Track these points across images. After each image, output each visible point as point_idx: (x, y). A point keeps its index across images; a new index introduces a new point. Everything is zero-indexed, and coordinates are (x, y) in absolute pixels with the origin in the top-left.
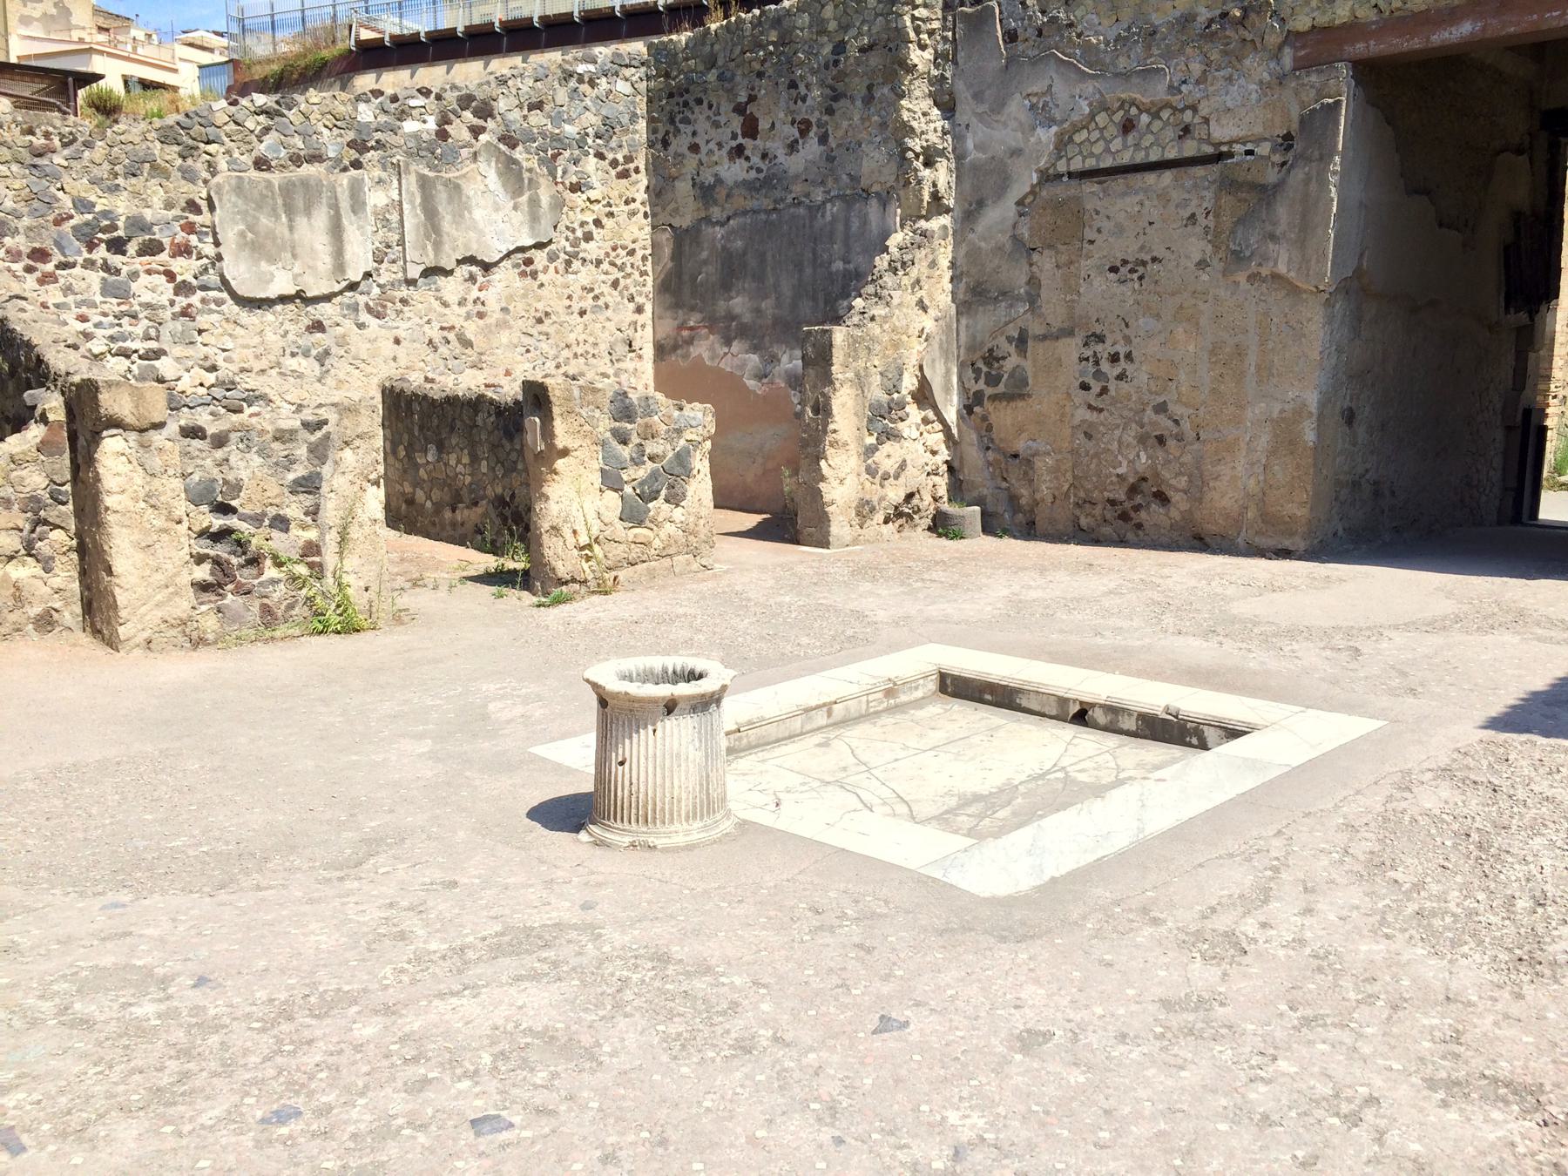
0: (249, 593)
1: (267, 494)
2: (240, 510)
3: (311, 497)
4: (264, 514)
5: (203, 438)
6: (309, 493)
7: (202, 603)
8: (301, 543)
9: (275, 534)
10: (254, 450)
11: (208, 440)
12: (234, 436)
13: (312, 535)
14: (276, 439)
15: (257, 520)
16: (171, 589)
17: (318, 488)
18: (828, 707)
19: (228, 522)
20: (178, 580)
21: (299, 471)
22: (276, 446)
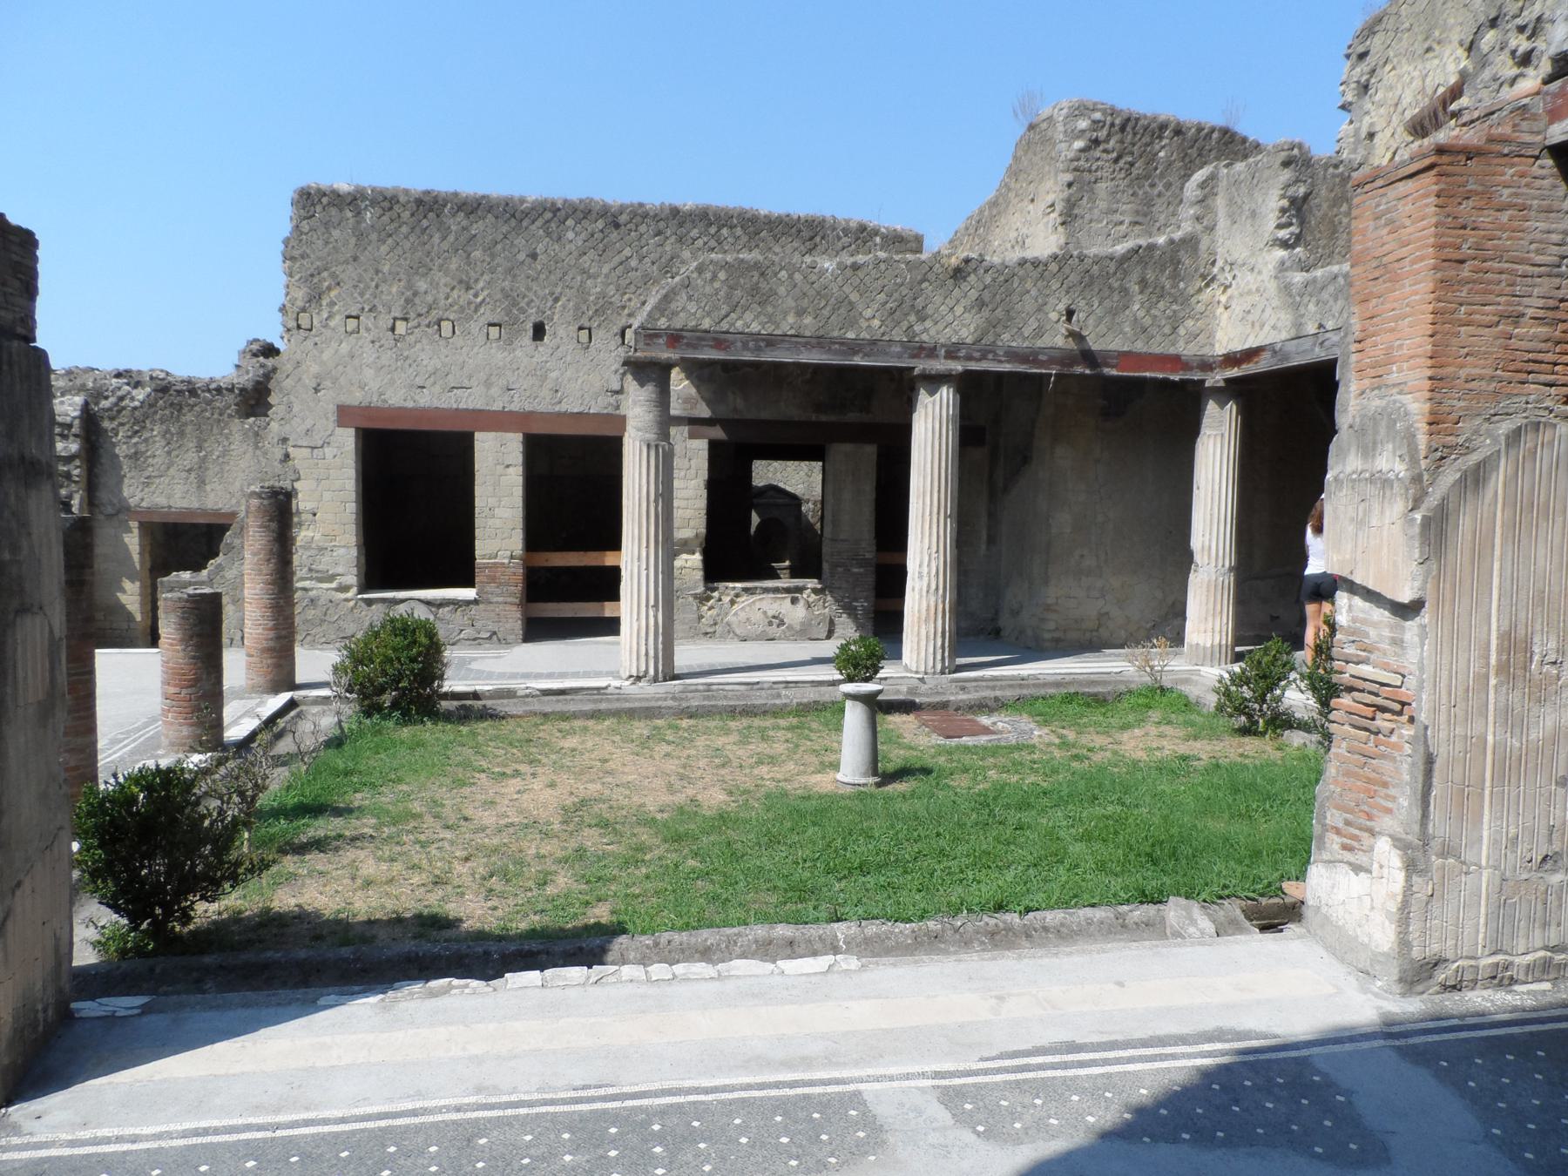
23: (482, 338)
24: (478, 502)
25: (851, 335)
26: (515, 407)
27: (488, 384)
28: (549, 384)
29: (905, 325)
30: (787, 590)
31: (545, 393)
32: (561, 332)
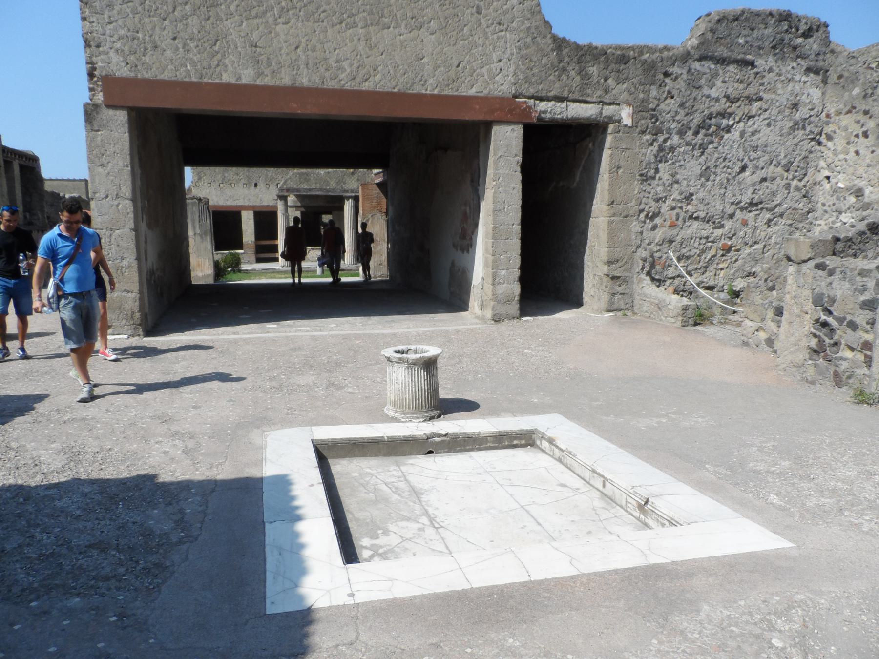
0: (830, 361)
1: (848, 307)
2: (835, 313)
3: (871, 313)
4: (845, 318)
5: (824, 270)
6: (870, 310)
7: (810, 359)
8: (862, 341)
9: (849, 331)
10: (847, 279)
11: (826, 271)
12: (838, 270)
13: (869, 337)
14: (859, 274)
15: (840, 320)
16: (797, 347)
17: (875, 309)
18: (605, 480)
19: (826, 318)
20: (800, 343)
21: (867, 296)
22: (858, 279)
24: (243, 228)
26: (251, 204)
27: (244, 199)
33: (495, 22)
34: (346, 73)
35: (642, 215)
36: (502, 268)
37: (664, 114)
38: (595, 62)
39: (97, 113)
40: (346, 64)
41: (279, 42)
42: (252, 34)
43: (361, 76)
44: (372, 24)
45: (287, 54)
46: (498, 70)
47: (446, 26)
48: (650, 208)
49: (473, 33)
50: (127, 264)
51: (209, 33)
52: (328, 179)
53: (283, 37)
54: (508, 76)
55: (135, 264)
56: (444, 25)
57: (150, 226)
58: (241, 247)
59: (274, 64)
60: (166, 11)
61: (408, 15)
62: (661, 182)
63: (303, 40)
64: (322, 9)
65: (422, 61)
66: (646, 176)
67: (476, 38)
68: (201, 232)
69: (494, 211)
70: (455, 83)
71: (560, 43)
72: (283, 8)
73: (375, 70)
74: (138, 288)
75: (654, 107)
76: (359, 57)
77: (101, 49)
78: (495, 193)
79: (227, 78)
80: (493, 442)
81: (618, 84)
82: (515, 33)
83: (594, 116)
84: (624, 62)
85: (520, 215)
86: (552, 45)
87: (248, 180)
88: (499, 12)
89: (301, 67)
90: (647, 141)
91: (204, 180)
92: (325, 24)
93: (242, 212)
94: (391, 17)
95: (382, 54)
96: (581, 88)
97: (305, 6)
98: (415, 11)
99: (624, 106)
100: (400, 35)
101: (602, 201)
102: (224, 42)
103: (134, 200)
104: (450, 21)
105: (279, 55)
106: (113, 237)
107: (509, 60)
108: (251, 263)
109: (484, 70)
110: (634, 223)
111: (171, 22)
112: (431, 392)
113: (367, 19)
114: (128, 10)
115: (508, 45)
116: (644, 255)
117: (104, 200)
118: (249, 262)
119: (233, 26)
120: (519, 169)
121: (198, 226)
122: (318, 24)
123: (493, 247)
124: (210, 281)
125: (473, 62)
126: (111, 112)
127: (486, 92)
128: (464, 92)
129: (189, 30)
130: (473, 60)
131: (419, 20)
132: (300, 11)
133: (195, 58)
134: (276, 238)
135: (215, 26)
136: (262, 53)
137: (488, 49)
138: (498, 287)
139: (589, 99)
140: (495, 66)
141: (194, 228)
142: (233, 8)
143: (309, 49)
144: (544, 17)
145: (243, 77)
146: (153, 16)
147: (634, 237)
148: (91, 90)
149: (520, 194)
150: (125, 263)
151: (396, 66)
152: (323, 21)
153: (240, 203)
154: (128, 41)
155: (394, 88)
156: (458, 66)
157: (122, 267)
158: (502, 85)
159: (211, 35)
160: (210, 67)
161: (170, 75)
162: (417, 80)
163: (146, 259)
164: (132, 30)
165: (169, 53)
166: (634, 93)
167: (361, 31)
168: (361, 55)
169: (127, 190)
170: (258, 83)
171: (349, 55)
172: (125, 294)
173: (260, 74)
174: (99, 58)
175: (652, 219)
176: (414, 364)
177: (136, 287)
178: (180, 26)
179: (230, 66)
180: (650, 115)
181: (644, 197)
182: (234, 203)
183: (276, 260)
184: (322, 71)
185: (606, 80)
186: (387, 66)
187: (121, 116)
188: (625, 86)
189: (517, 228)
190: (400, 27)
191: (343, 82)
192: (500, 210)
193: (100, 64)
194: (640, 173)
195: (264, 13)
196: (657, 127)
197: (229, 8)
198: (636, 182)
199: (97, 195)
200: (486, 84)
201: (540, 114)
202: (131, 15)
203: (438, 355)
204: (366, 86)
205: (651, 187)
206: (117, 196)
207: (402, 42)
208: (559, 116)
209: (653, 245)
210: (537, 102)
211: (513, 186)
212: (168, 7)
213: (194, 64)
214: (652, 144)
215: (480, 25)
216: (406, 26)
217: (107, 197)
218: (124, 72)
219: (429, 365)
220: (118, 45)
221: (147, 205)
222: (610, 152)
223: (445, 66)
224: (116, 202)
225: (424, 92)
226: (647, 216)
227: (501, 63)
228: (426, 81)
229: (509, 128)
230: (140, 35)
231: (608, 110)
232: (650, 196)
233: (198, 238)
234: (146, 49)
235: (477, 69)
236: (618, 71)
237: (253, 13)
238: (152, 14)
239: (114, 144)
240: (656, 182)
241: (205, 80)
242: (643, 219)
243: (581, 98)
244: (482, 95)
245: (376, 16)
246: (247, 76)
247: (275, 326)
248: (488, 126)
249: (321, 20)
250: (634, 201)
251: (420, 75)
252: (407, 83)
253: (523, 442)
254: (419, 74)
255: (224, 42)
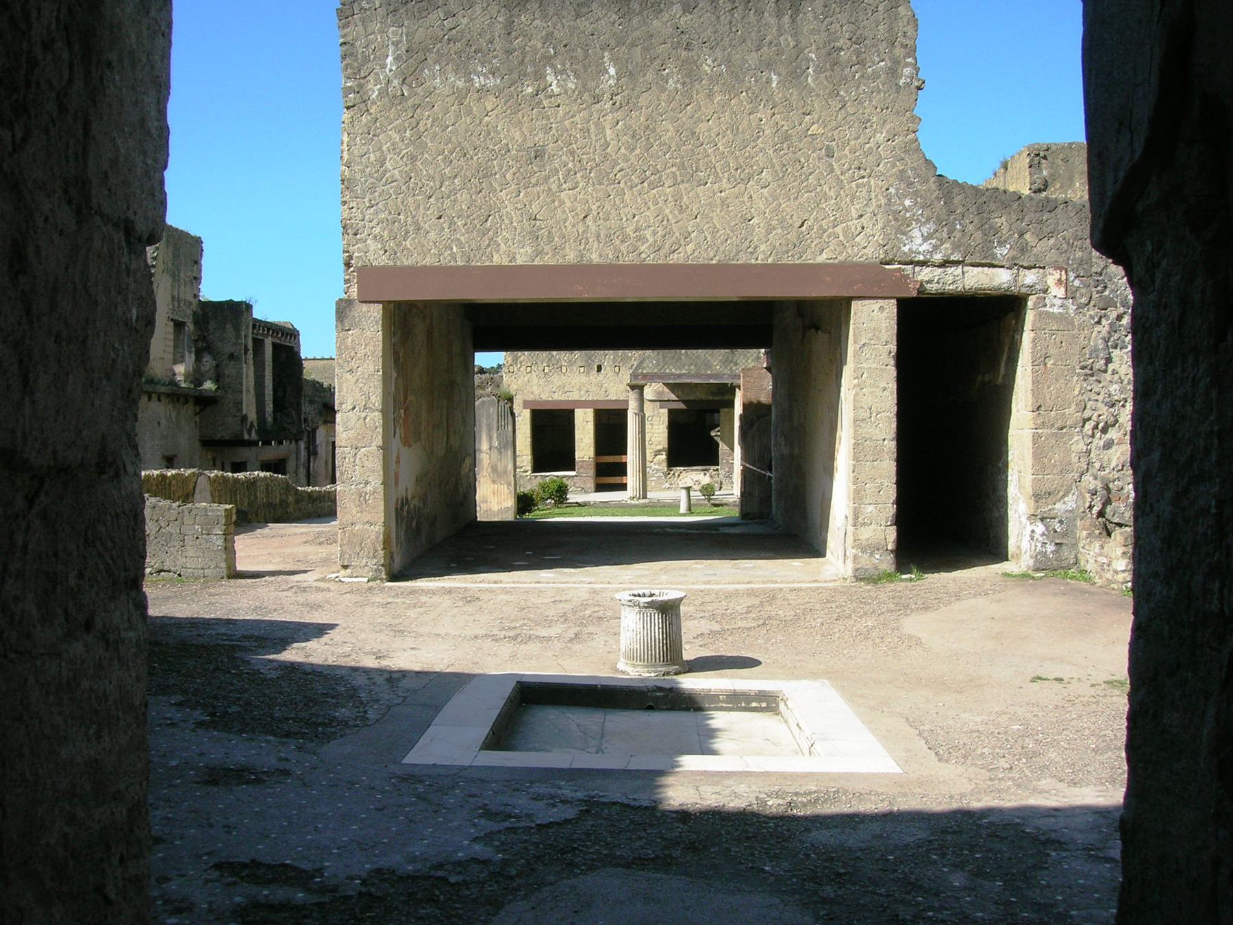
23: (578, 372)
25: (709, 372)
26: (590, 399)
27: (580, 390)
28: (603, 389)
29: (729, 368)
30: (703, 470)
31: (602, 392)
32: (608, 368)
33: (853, 167)
34: (648, 244)
35: (1089, 426)
36: (868, 502)
37: (1115, 280)
38: (1004, 211)
39: (350, 310)
40: (648, 234)
41: (564, 212)
42: (531, 205)
43: (667, 246)
44: (683, 181)
45: (573, 226)
46: (859, 229)
47: (783, 176)
48: (1100, 416)
49: (822, 182)
50: (372, 489)
51: (480, 209)
52: (709, 358)
53: (568, 204)
54: (873, 236)
55: (381, 489)
56: (781, 175)
57: (406, 442)
58: (571, 467)
59: (556, 239)
60: (432, 188)
61: (731, 165)
62: (1116, 377)
63: (594, 207)
64: (618, 168)
65: (751, 222)
66: (1091, 369)
67: (826, 188)
68: (499, 444)
69: (855, 421)
70: (796, 249)
71: (947, 187)
72: (569, 171)
73: (686, 238)
74: (383, 520)
75: (1099, 270)
76: (665, 223)
77: (358, 236)
78: (856, 394)
79: (499, 259)
80: (727, 702)
81: (1040, 240)
82: (882, 178)
83: (1005, 285)
84: (1048, 209)
85: (894, 425)
86: (937, 192)
87: (587, 361)
88: (857, 154)
89: (591, 240)
90: (1092, 317)
91: (521, 363)
92: (622, 185)
93: (576, 410)
94: (708, 170)
95: (696, 218)
96: (983, 247)
97: (597, 165)
98: (741, 160)
99: (1048, 270)
100: (721, 192)
101: (1026, 406)
102: (497, 217)
103: (384, 412)
104: (789, 170)
105: (563, 227)
106: (358, 456)
107: (875, 215)
108: (586, 492)
109: (839, 229)
110: (1076, 438)
111: (437, 199)
112: (667, 644)
113: (676, 175)
114: (391, 191)
115: (873, 195)
116: (1091, 487)
117: (351, 412)
118: (584, 491)
119: (508, 197)
120: (892, 362)
121: (495, 435)
122: (613, 187)
123: (854, 472)
124: (510, 517)
125: (823, 220)
126: (365, 307)
127: (841, 258)
128: (810, 259)
129: (457, 207)
130: (823, 217)
131: (747, 171)
132: (590, 173)
133: (462, 238)
134: (623, 451)
135: (487, 199)
136: (543, 226)
137: (843, 202)
138: (862, 529)
139: (996, 263)
140: (854, 224)
141: (490, 438)
142: (509, 176)
143: (602, 217)
144: (924, 155)
145: (518, 256)
146: (418, 195)
147: (1075, 460)
148: (347, 281)
149: (895, 396)
150: (369, 488)
151: (714, 232)
152: (619, 183)
153: (574, 396)
154: (388, 225)
155: (712, 260)
156: (802, 225)
157: (366, 493)
158: (864, 248)
159: (483, 211)
160: (479, 248)
161: (433, 261)
162: (744, 246)
163: (396, 484)
164: (393, 213)
165: (433, 235)
166: (1066, 251)
167: (668, 190)
168: (668, 220)
169: (376, 400)
170: (536, 263)
171: (652, 221)
172: (367, 526)
173: (539, 253)
174: (356, 247)
175: (1104, 431)
176: (646, 607)
177: (380, 517)
178: (447, 202)
179: (502, 245)
180: (1094, 280)
181: (1089, 400)
182: (563, 398)
183: (623, 487)
184: (617, 243)
185: (1021, 235)
186: (703, 232)
187: (375, 312)
188: (1052, 241)
189: (891, 446)
190: (721, 181)
191: (643, 256)
192: (864, 420)
193: (356, 254)
194: (1082, 364)
195: (546, 179)
196: (1107, 297)
197: (505, 176)
198: (1075, 378)
199: (344, 406)
200: (842, 247)
201: (921, 284)
202: (394, 197)
203: (681, 599)
204: (675, 259)
205: (1101, 385)
206: (365, 407)
207: (723, 201)
208: (951, 287)
209: (1107, 471)
210: (917, 269)
211: (883, 385)
212: (434, 181)
213: (460, 245)
214: (1099, 322)
215: (832, 171)
216: (729, 179)
217: (354, 408)
218: (382, 260)
219: (668, 610)
220: (377, 230)
221: (403, 415)
222: (1032, 334)
223: (782, 228)
224: (363, 415)
225: (753, 261)
226: (1096, 427)
227: (862, 219)
228: (756, 247)
229: (875, 305)
230: (402, 217)
231: (1030, 277)
232: (1100, 398)
233: (495, 454)
234: (407, 232)
235: (829, 228)
236: (1040, 222)
237: (533, 180)
238: (417, 192)
239: (366, 345)
240: (1108, 376)
241: (473, 264)
242: (1090, 433)
243: (983, 262)
244: (836, 261)
245: (689, 170)
246: (523, 256)
247: (552, 575)
248: (848, 301)
249: (617, 181)
250: (1073, 407)
251: (748, 241)
252: (730, 252)
253: (764, 705)
254: (746, 240)
255: (497, 217)
